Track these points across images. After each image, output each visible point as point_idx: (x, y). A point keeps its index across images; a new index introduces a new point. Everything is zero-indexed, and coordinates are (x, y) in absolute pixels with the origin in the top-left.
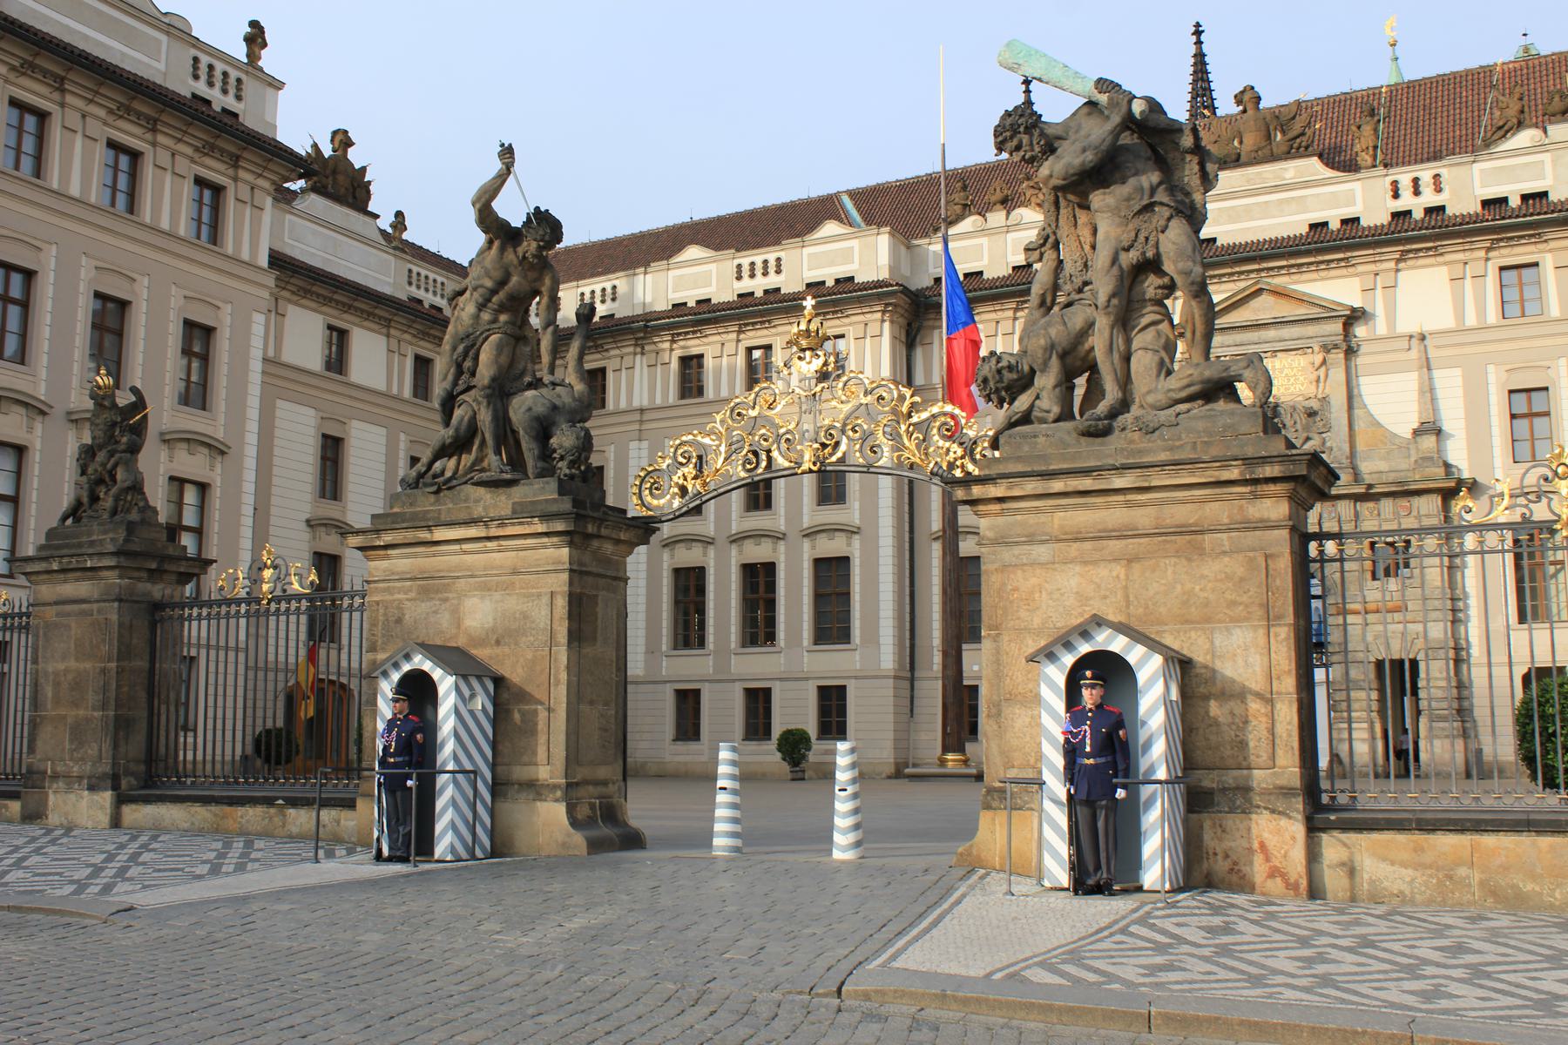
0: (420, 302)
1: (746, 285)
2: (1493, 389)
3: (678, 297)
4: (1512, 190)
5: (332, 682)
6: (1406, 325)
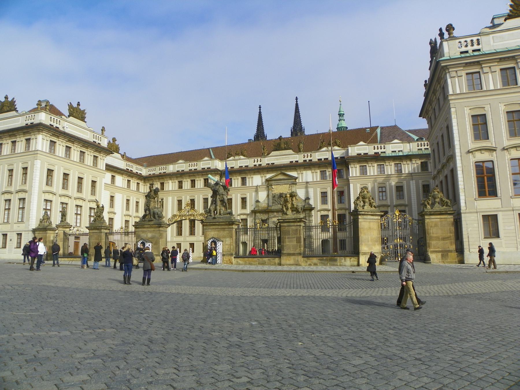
0: (128, 169)
1: (190, 168)
2: (318, 192)
3: (178, 169)
4: (323, 158)
5: (112, 242)
6: (304, 181)
